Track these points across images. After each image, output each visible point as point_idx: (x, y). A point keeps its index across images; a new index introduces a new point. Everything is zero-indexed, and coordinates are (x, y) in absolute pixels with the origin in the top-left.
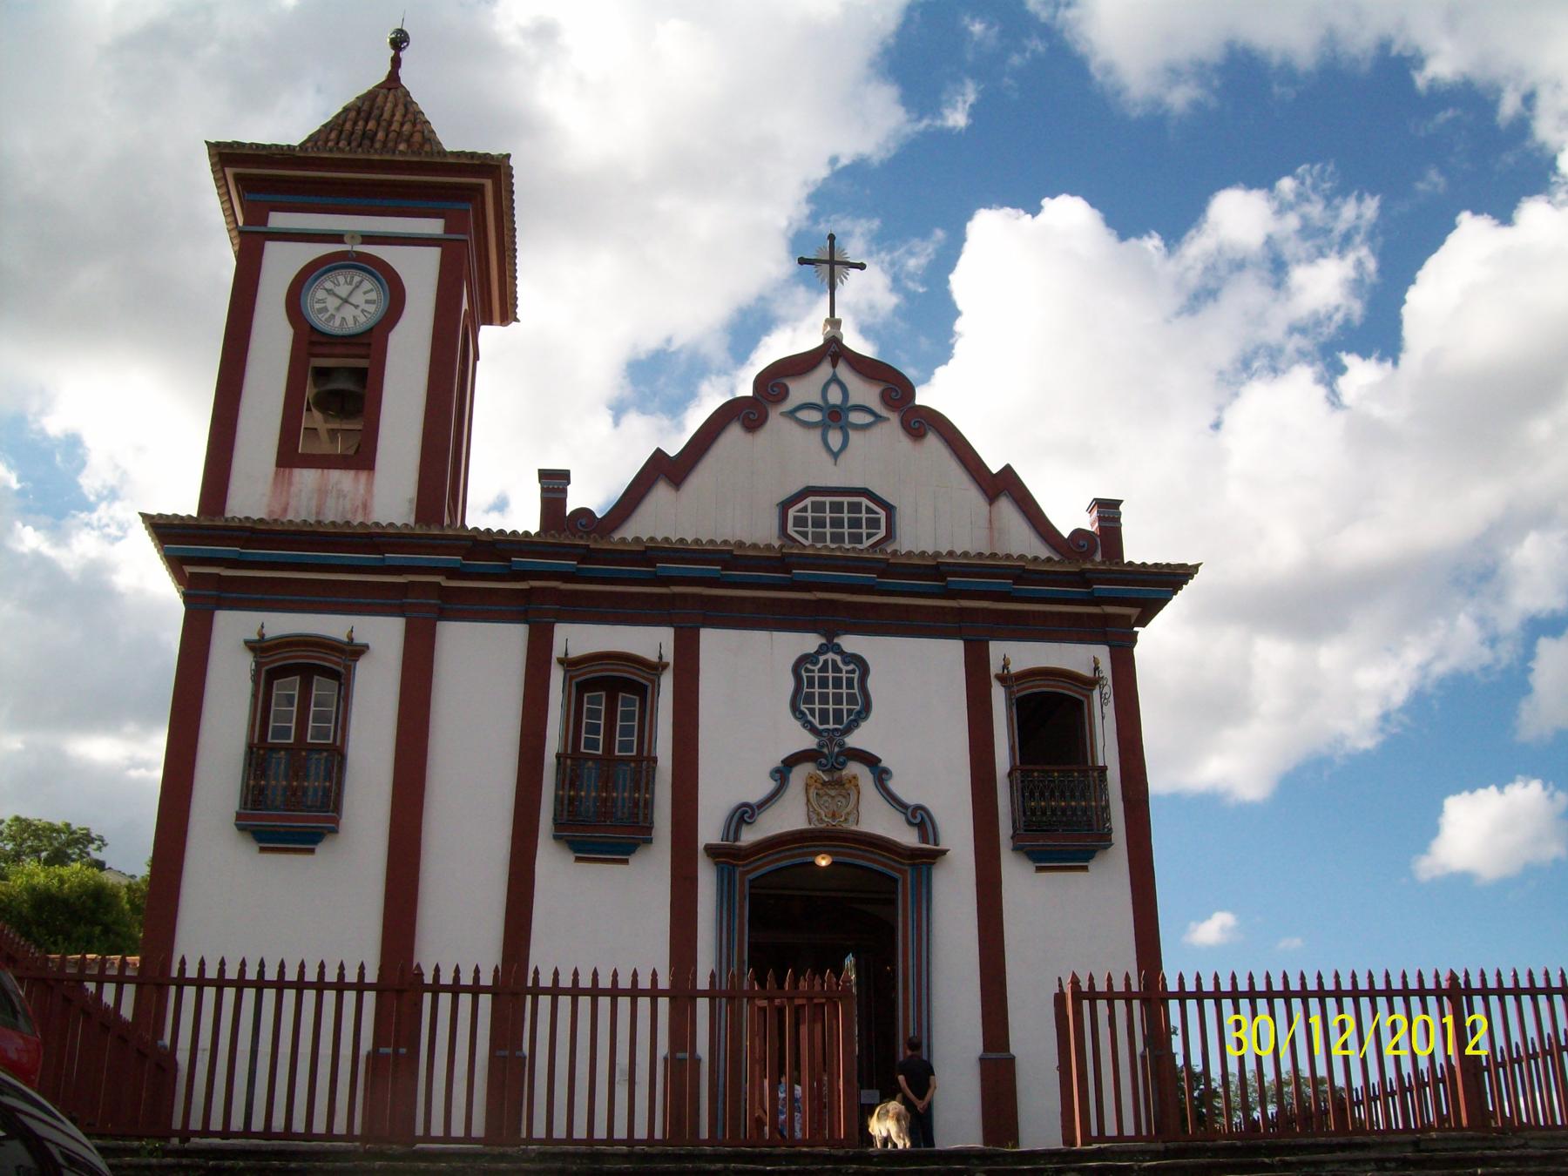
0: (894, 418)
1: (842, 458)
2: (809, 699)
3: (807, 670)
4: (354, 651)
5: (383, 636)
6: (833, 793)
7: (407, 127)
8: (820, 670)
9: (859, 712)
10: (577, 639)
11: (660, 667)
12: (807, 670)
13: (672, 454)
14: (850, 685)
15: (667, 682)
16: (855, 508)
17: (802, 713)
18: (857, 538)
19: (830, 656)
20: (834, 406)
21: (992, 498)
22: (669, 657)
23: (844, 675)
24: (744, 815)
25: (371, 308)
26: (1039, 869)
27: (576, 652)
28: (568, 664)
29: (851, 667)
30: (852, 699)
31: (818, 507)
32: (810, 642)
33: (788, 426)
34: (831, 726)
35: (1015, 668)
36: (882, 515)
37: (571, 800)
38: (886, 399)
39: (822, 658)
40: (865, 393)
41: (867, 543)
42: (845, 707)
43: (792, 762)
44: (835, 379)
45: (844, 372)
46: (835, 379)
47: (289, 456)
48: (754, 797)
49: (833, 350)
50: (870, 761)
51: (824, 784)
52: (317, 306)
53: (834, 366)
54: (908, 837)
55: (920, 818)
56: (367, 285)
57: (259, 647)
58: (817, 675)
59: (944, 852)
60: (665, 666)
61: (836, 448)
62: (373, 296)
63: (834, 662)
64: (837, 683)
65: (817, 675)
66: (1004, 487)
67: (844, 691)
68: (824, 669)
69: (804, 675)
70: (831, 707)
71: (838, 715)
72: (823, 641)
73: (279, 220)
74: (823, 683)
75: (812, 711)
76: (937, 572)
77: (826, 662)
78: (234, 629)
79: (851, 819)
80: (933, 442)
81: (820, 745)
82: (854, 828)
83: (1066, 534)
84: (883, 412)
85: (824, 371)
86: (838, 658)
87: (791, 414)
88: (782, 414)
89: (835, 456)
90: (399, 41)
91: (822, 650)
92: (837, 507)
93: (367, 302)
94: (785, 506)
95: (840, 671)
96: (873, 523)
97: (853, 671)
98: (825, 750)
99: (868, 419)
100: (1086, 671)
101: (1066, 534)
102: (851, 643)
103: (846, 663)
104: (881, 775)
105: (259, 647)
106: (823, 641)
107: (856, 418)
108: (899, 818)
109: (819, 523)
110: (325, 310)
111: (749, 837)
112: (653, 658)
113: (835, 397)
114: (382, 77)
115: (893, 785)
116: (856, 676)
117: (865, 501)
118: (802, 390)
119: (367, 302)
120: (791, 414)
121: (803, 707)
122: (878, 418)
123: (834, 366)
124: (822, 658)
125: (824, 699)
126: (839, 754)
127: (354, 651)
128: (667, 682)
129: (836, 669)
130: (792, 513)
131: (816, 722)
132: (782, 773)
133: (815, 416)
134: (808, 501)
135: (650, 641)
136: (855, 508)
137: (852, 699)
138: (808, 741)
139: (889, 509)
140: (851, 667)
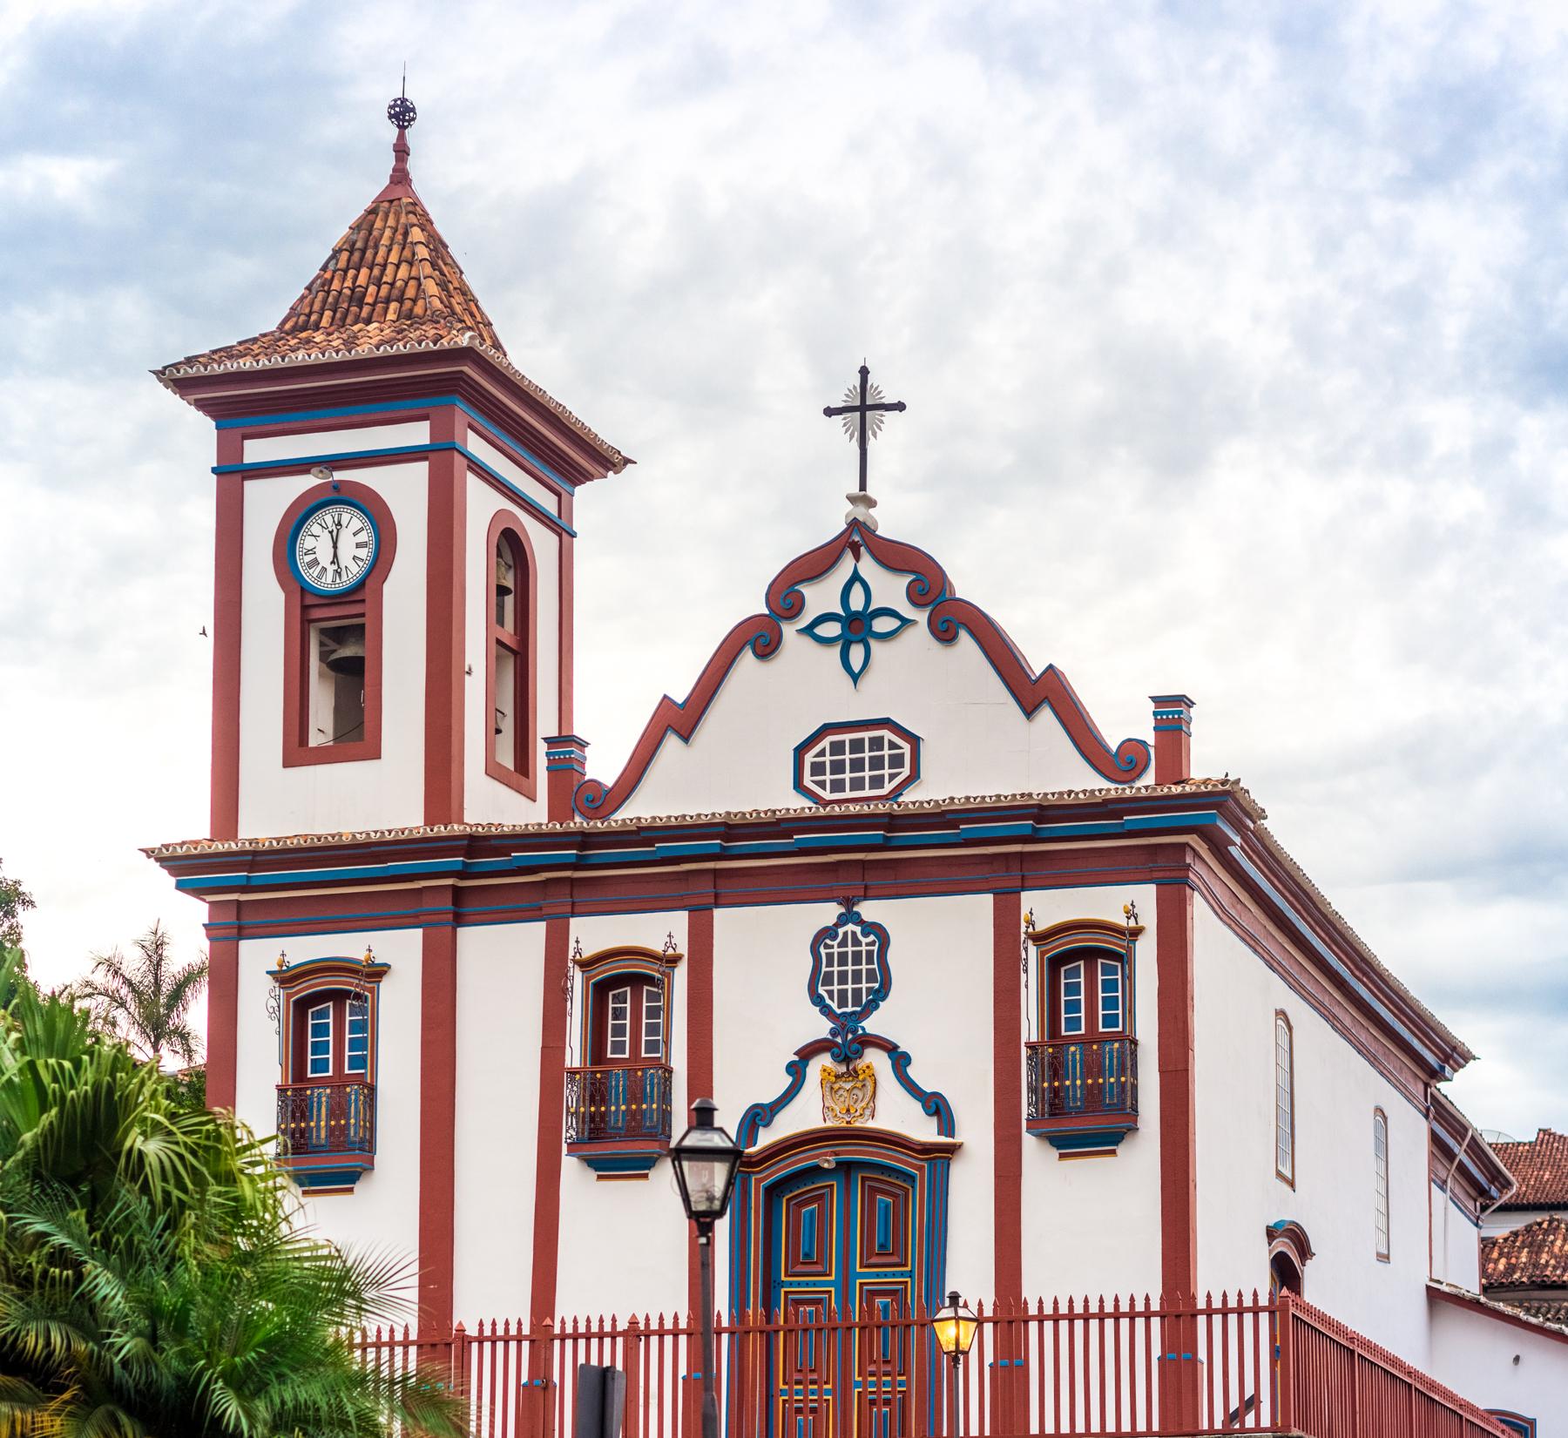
0: (922, 617)
1: (862, 683)
2: (828, 980)
3: (827, 946)
4: (377, 972)
5: (401, 950)
6: (848, 1086)
7: (403, 272)
8: (840, 946)
9: (878, 991)
10: (594, 934)
11: (674, 960)
12: (827, 946)
13: (680, 700)
14: (870, 961)
15: (681, 975)
16: (877, 743)
17: (821, 997)
18: (877, 782)
19: (850, 927)
20: (857, 613)
21: (1029, 712)
22: (683, 949)
23: (864, 948)
24: (757, 1117)
25: (363, 553)
26: (1062, 1156)
27: (587, 953)
28: (585, 965)
29: (872, 938)
30: (871, 976)
31: (837, 748)
32: (828, 913)
33: (807, 642)
34: (850, 1009)
35: (1041, 926)
36: (906, 748)
37: (592, 1117)
38: (916, 596)
39: (841, 931)
40: (890, 590)
41: (889, 787)
42: (864, 985)
43: (807, 1053)
44: (856, 577)
45: (868, 567)
46: (856, 577)
47: (298, 751)
48: (768, 1098)
49: (858, 537)
50: (890, 1048)
51: (837, 1077)
52: (308, 559)
53: (857, 557)
54: (924, 1130)
55: (936, 1106)
56: (356, 524)
57: (285, 977)
58: (836, 950)
59: (960, 1146)
60: (674, 960)
61: (856, 667)
62: (363, 537)
63: (854, 933)
64: (857, 958)
65: (836, 950)
66: (1040, 692)
67: (864, 967)
68: (843, 944)
69: (823, 951)
70: (850, 987)
71: (857, 992)
72: (842, 910)
73: (257, 451)
74: (843, 959)
75: (830, 993)
76: (943, 818)
77: (845, 934)
78: (260, 958)
79: (868, 1112)
80: (965, 640)
81: (834, 1033)
82: (871, 1124)
83: (1113, 746)
84: (907, 611)
85: (846, 566)
86: (858, 929)
87: (808, 630)
88: (800, 631)
89: (855, 678)
90: (402, 113)
91: (842, 920)
92: (857, 746)
93: (358, 546)
94: (800, 751)
95: (859, 943)
96: (897, 761)
97: (873, 943)
98: (839, 1040)
99: (897, 623)
100: (1121, 920)
101: (1113, 746)
102: (870, 910)
103: (865, 935)
104: (900, 1061)
105: (285, 977)
106: (842, 910)
107: (882, 625)
108: (916, 1107)
109: (838, 767)
110: (315, 562)
111: (766, 1138)
112: (658, 948)
113: (857, 602)
114: (379, 182)
115: (912, 1072)
116: (876, 948)
117: (887, 735)
118: (821, 597)
119: (358, 546)
120: (808, 630)
121: (821, 990)
122: (906, 622)
123: (857, 557)
124: (841, 931)
125: (843, 978)
126: (853, 1041)
127: (377, 972)
128: (681, 975)
129: (856, 942)
130: (809, 758)
131: (834, 1006)
132: (797, 1070)
133: (832, 630)
134: (825, 743)
135: (660, 930)
136: (877, 743)
137: (871, 976)
138: (822, 1028)
139: (914, 741)
140: (872, 938)
